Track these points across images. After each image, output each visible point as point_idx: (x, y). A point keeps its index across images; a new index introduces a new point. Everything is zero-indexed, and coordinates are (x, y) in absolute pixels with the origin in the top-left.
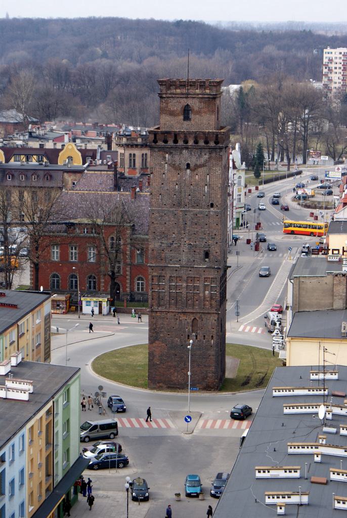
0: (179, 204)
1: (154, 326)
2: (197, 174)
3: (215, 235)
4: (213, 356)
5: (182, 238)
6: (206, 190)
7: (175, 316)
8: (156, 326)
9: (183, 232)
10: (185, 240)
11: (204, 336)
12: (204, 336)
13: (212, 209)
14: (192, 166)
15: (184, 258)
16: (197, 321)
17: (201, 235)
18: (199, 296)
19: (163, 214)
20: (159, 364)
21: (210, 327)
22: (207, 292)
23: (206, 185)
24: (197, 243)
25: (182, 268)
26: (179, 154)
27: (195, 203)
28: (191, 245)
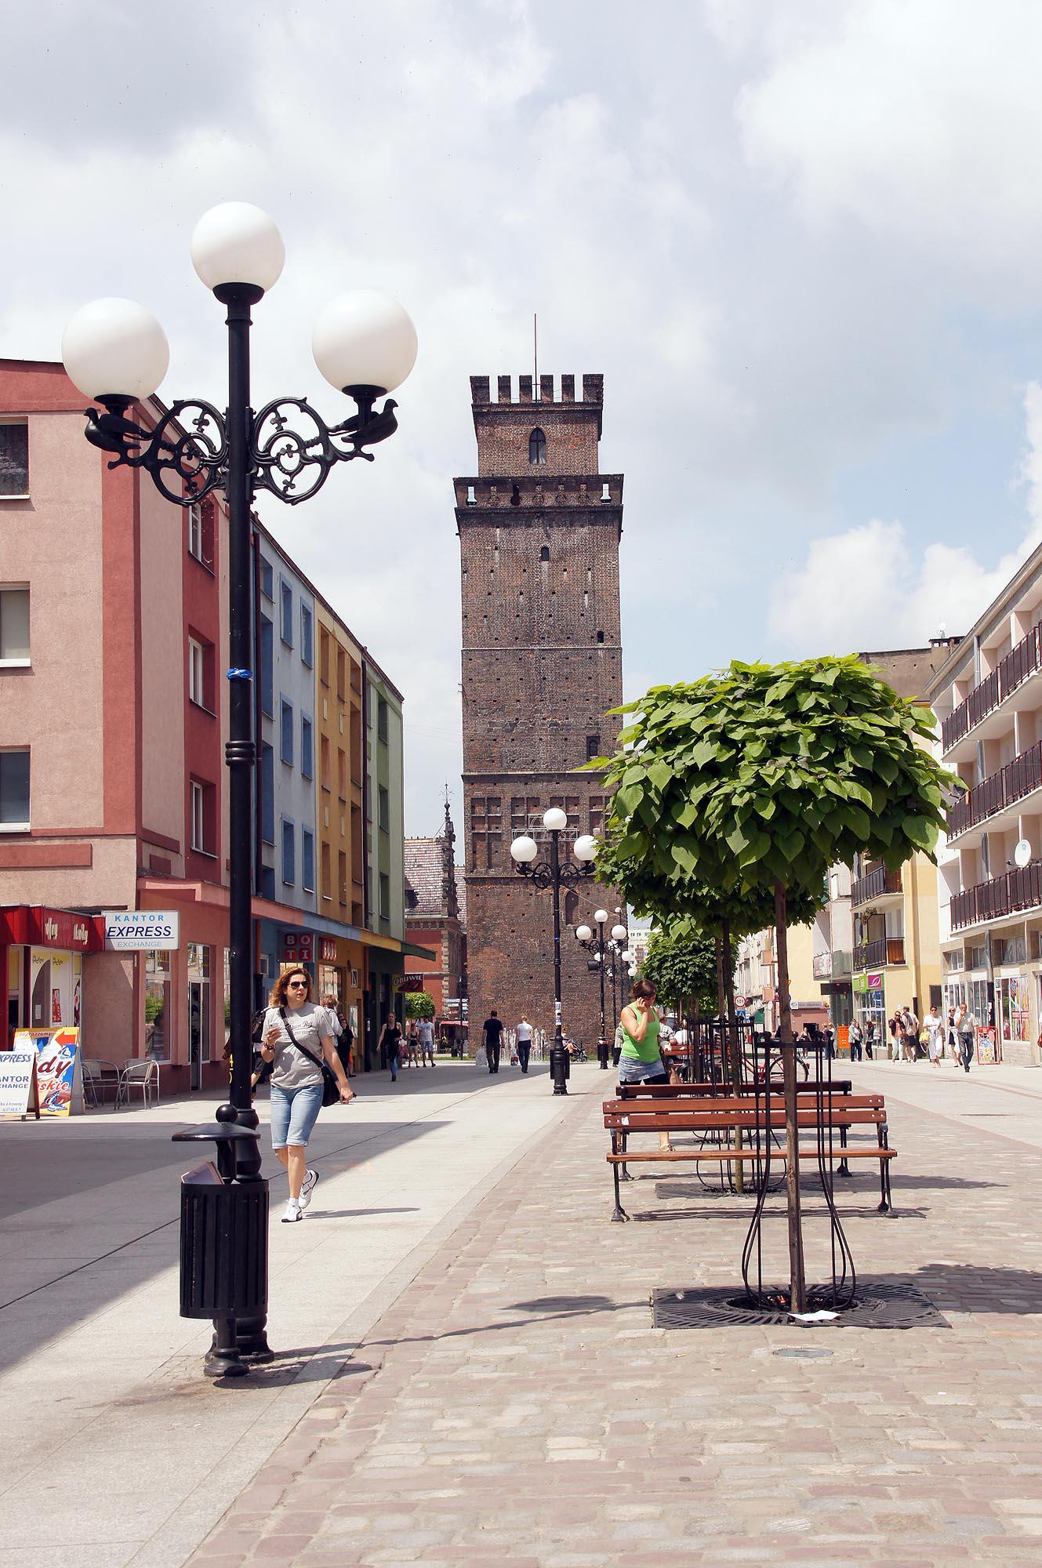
0: (529, 637)
1: (480, 913)
2: (565, 570)
6: (586, 604)
8: (484, 913)
13: (601, 645)
14: (553, 555)
15: (542, 754)
20: (492, 1002)
23: (586, 592)
24: (571, 720)
27: (562, 632)
28: (556, 724)
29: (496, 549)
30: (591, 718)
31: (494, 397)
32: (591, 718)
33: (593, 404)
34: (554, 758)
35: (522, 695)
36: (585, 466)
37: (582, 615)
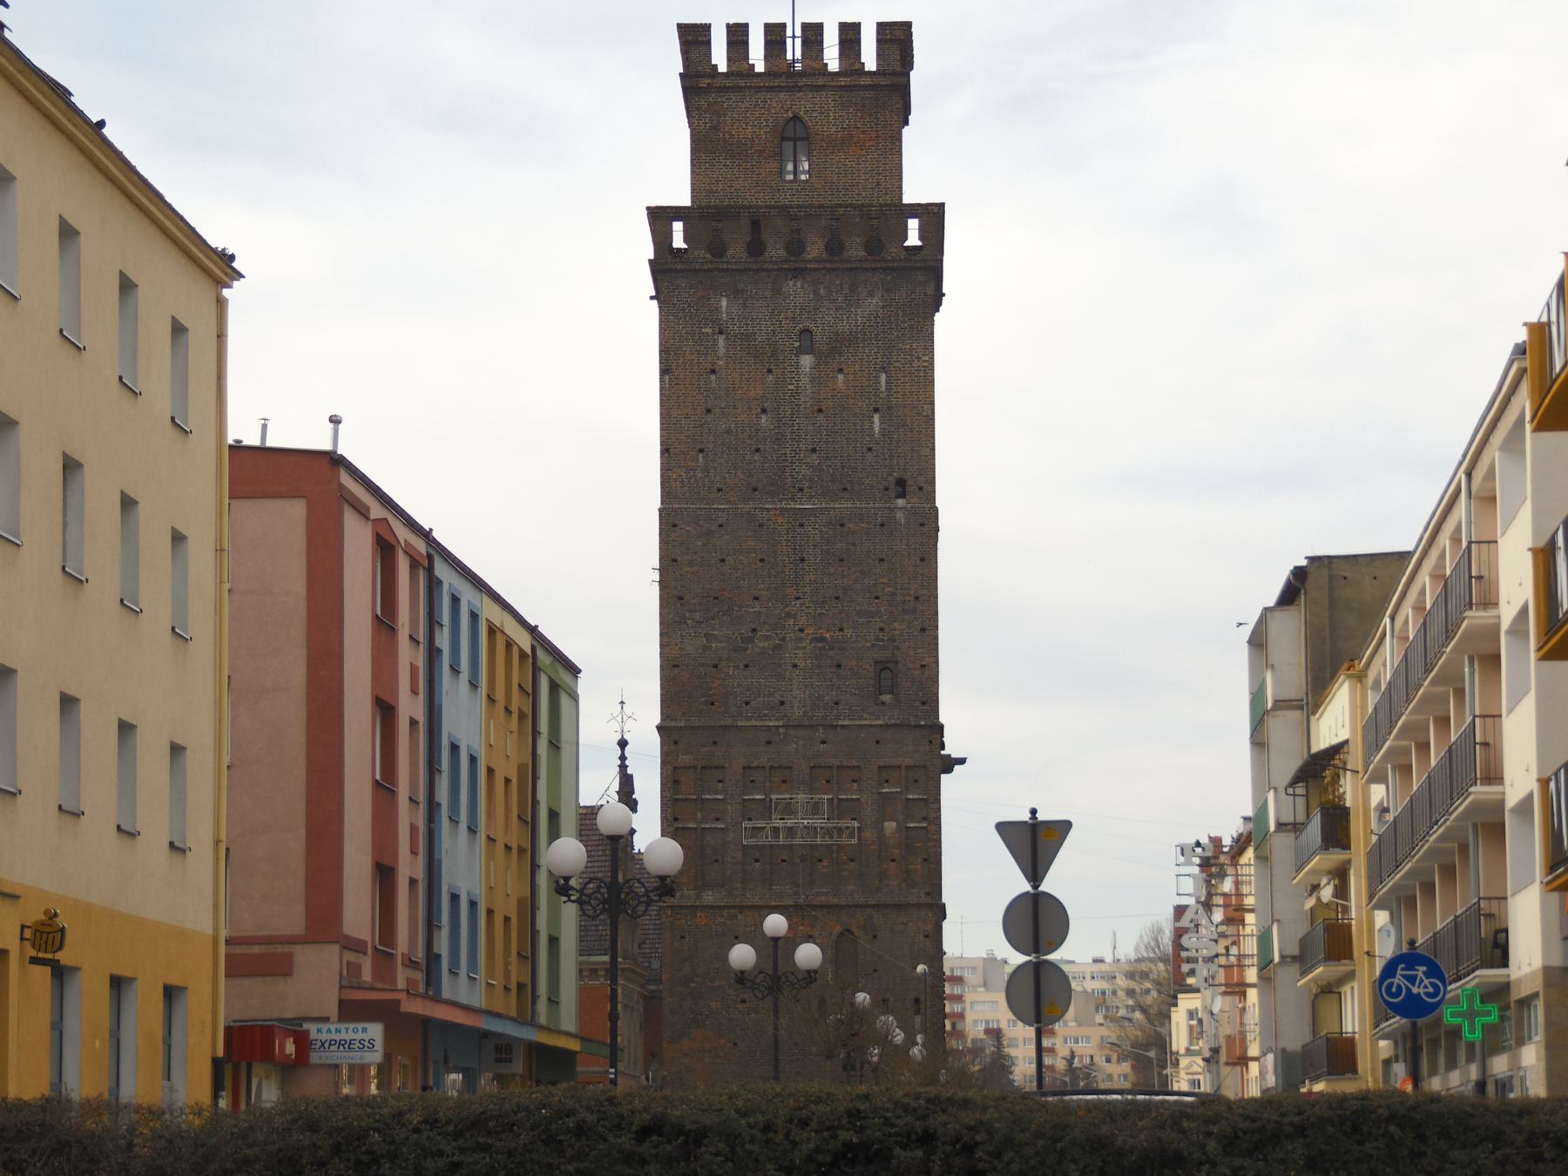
2: (841, 370)
3: (917, 598)
5: (788, 615)
9: (791, 591)
10: (803, 621)
13: (901, 502)
19: (715, 527)
23: (876, 410)
25: (793, 732)
26: (768, 294)
28: (822, 639)
29: (721, 333)
30: (882, 630)
31: (719, 57)
32: (882, 630)
33: (894, 74)
36: (878, 184)
37: (870, 449)
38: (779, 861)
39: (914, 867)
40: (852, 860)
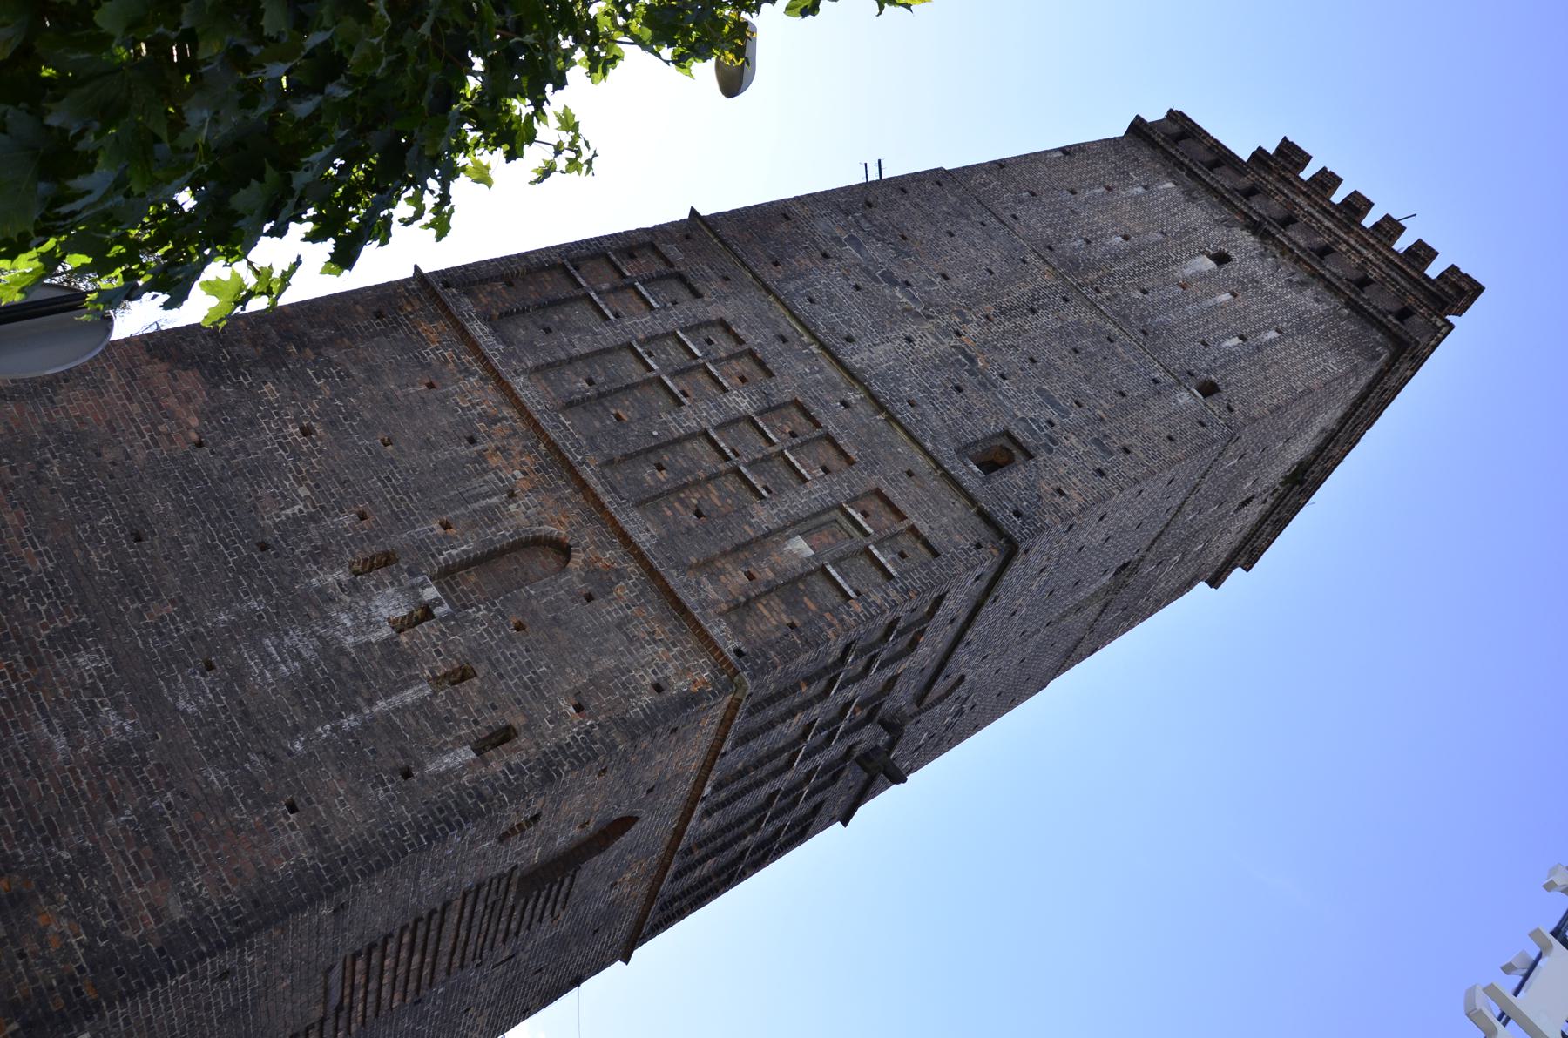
1: (317, 334)
4: (316, 836)
7: (494, 420)
11: (463, 675)
12: (463, 675)
16: (563, 567)
17: (1056, 389)
18: (742, 511)
21: (576, 678)
22: (800, 547)
28: (972, 360)
34: (896, 379)
35: (961, 281)
38: (614, 411)
39: (766, 613)
40: (698, 514)
